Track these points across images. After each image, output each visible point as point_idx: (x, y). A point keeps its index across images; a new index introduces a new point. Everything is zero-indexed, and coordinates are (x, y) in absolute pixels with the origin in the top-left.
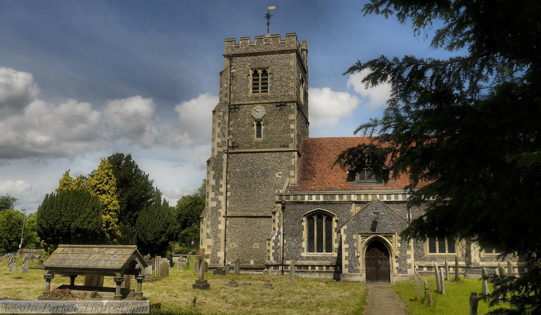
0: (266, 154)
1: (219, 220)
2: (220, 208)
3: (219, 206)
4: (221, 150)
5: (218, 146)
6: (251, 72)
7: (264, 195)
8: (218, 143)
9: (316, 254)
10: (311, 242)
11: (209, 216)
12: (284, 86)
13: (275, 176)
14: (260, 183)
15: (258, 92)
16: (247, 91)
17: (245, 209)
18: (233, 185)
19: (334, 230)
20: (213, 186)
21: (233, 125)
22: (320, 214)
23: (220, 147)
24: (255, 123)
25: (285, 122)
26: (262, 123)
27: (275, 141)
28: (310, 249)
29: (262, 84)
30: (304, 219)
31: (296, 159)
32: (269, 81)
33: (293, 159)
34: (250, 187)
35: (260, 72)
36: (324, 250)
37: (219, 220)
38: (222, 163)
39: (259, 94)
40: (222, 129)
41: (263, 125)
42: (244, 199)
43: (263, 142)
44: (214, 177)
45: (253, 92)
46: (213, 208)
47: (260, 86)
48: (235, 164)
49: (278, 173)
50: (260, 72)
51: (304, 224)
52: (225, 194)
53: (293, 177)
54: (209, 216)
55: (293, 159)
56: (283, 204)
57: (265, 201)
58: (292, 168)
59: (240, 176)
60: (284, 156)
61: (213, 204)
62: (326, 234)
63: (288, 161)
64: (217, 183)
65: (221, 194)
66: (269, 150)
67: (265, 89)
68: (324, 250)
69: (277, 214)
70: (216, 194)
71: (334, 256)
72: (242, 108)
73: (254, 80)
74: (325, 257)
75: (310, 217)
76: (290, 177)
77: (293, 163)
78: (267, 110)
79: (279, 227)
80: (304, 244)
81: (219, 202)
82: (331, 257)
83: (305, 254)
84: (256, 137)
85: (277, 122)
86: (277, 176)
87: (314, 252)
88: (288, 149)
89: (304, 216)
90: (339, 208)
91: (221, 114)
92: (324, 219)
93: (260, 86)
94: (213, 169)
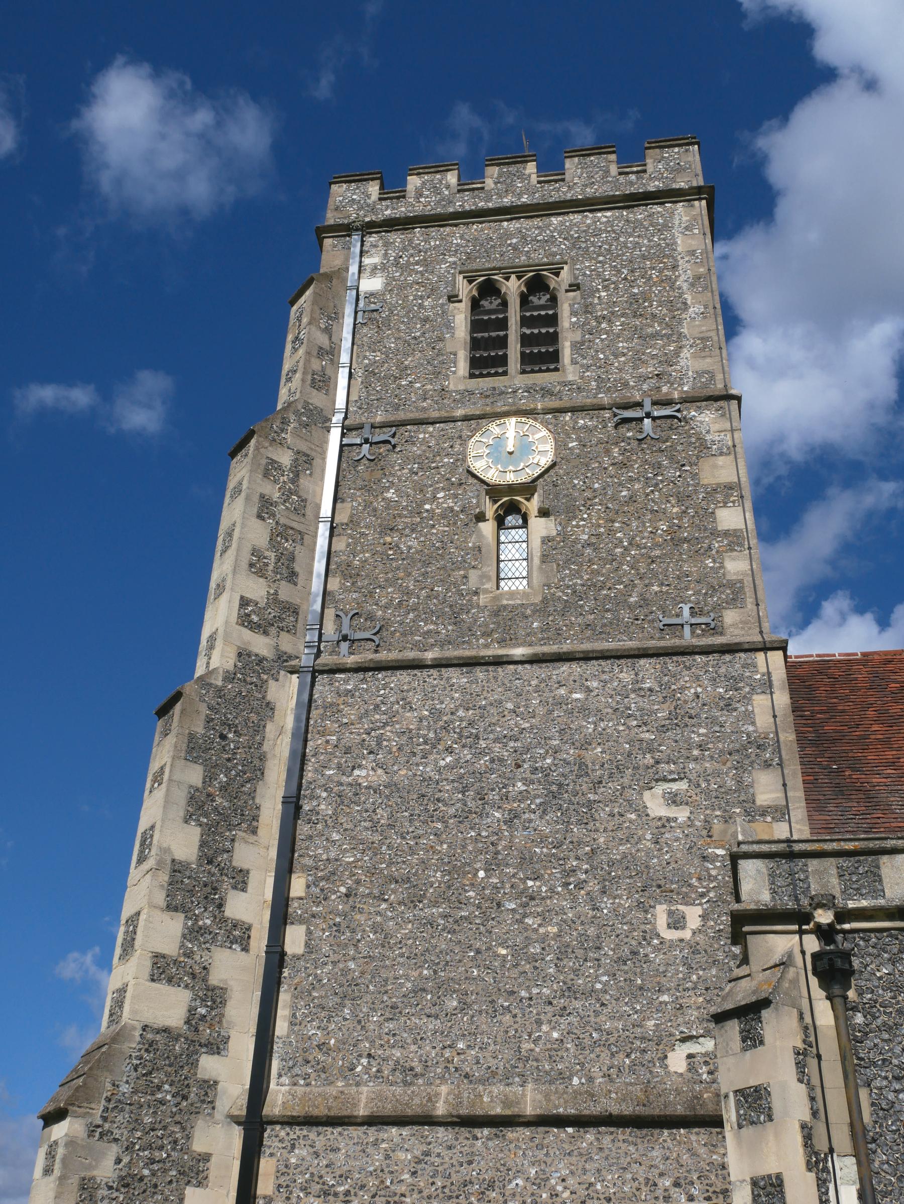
0: (565, 668)
1: (199, 1145)
2: (217, 1047)
3: (202, 1032)
4: (261, 645)
5: (245, 620)
6: (465, 289)
7: (563, 953)
8: (244, 602)
11: (115, 1104)
12: (654, 336)
13: (642, 812)
14: (526, 860)
15: (505, 373)
16: (439, 369)
17: (413, 1055)
18: (326, 876)
20: (177, 869)
21: (353, 522)
23: (261, 628)
24: (490, 510)
25: (681, 498)
26: (533, 506)
27: (621, 601)
29: (525, 340)
31: (782, 699)
32: (566, 319)
33: (760, 702)
34: (450, 895)
35: (513, 287)
37: (199, 1145)
38: (259, 729)
39: (515, 378)
40: (280, 534)
41: (544, 513)
42: (406, 977)
43: (543, 609)
44: (197, 806)
45: (472, 376)
46: (156, 1038)
47: (514, 350)
48: (351, 738)
49: (660, 788)
50: (513, 287)
52: (260, 941)
53: (781, 812)
54: (115, 1104)
55: (760, 702)
56: (825, 933)
57: (570, 991)
58: (754, 751)
59: (382, 814)
60: (696, 683)
61: (170, 1007)
63: (728, 706)
64: (213, 852)
65: (239, 936)
66: (587, 646)
67: (542, 354)
69: (780, 1031)
70: (194, 933)
72: (410, 441)
73: (476, 326)
76: (753, 812)
77: (763, 721)
78: (560, 445)
79: (819, 1162)
81: (213, 998)
84: (490, 585)
85: (632, 499)
86: (655, 804)
88: (719, 640)
91: (285, 459)
93: (514, 350)
94: (194, 750)
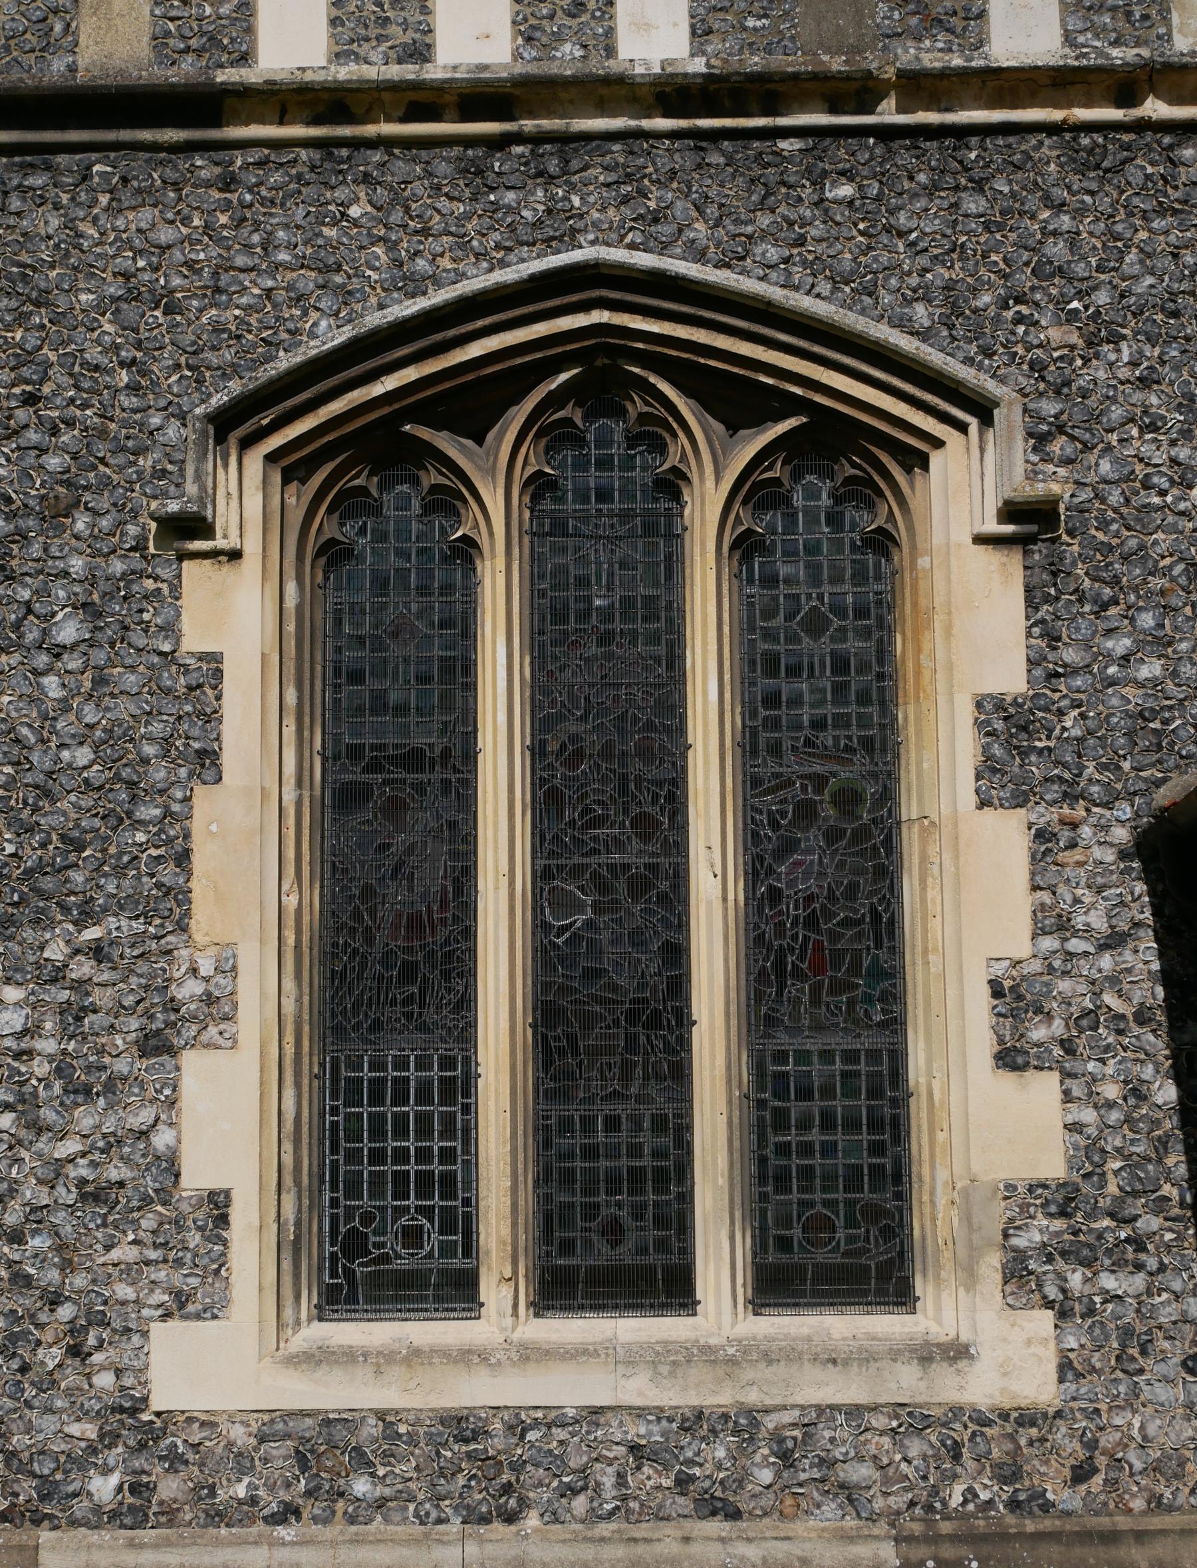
9: (506, 1353)
10: (404, 1056)
19: (942, 757)
22: (600, 382)
28: (377, 1236)
30: (243, 496)
36: (719, 1253)
51: (236, 615)
62: (764, 853)
68: (719, 1253)
71: (980, 1387)
74: (744, 1425)
75: (368, 454)
80: (229, 1115)
82: (912, 1420)
83: (231, 1358)
87: (458, 1291)
89: (231, 425)
90: (1067, 230)
92: (706, 505)
